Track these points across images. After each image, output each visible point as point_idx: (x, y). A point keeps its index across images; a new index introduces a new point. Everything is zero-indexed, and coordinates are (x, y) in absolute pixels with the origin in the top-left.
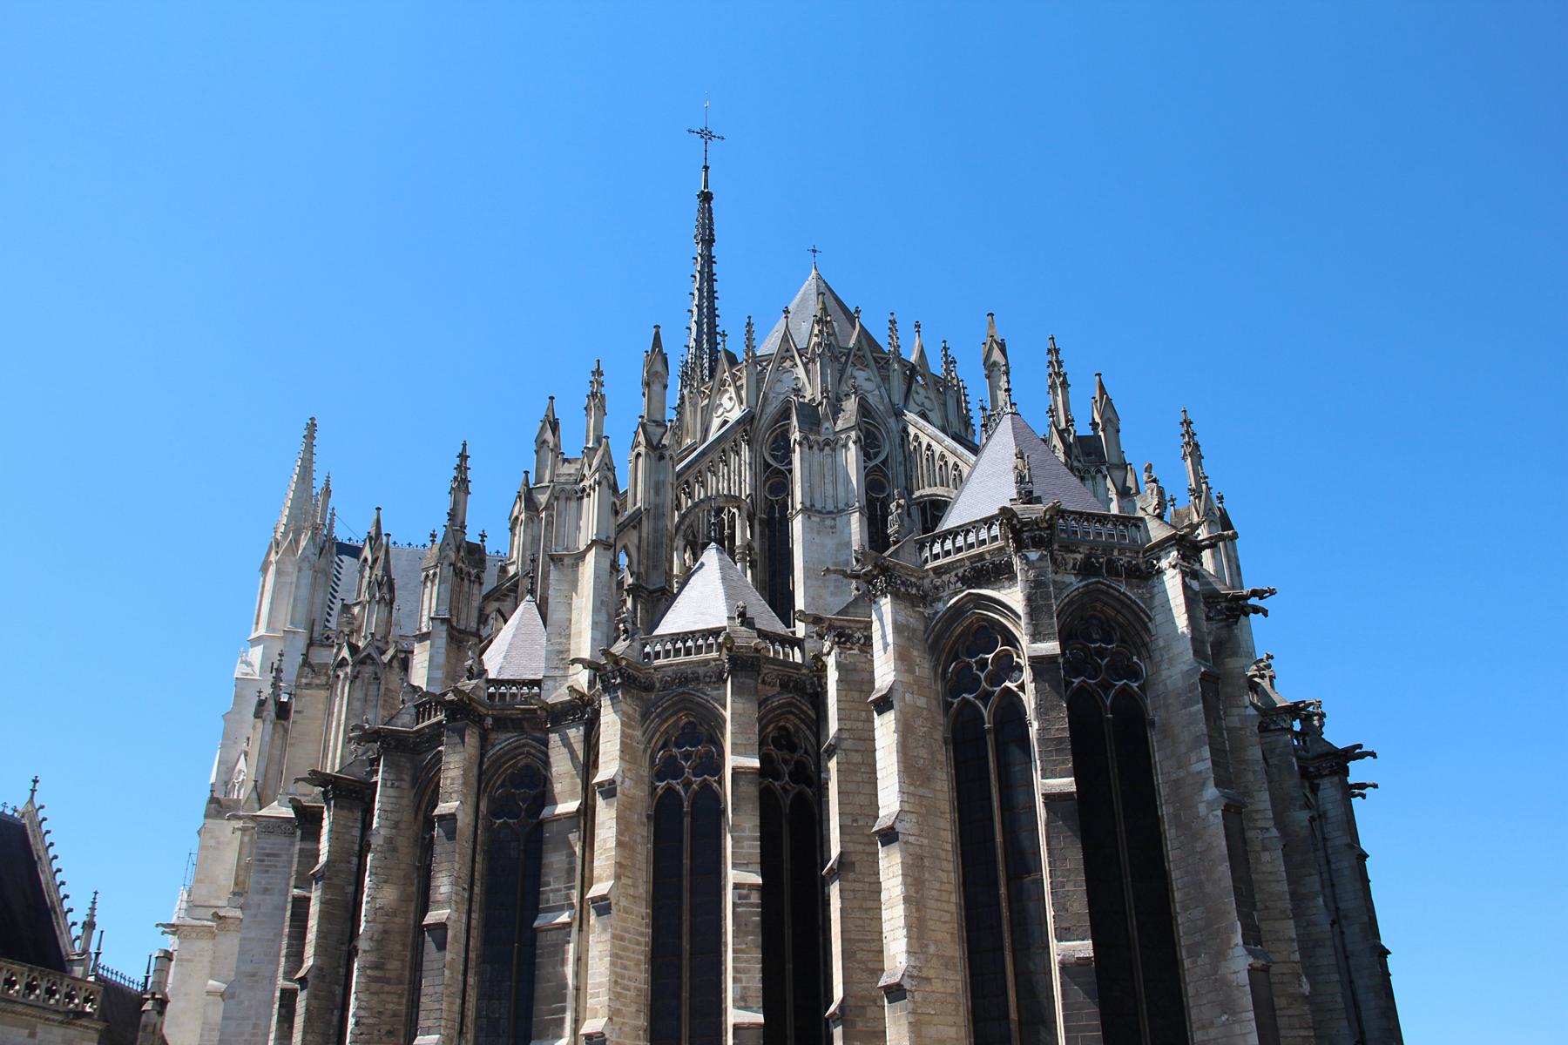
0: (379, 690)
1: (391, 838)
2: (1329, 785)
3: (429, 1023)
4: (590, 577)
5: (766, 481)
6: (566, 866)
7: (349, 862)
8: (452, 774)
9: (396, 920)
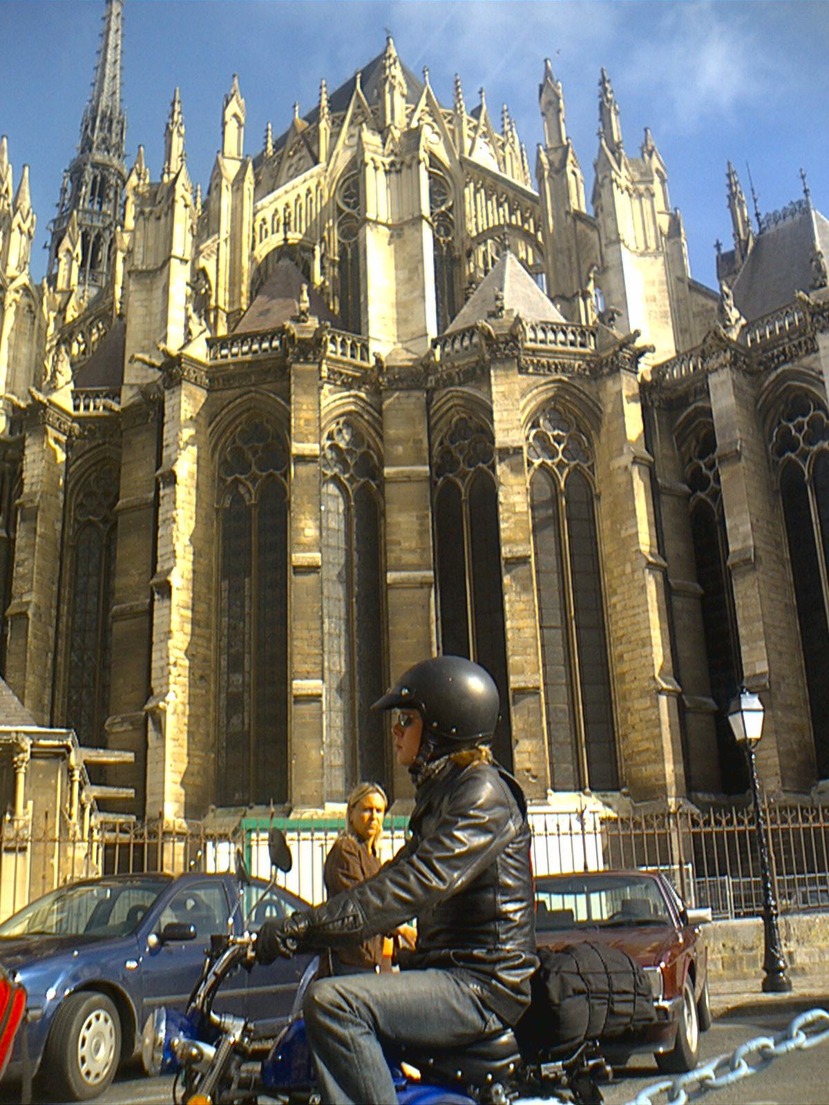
0: (33, 323)
3: (307, 667)
6: (416, 527)
7: (57, 497)
8: (304, 415)
9: (202, 560)
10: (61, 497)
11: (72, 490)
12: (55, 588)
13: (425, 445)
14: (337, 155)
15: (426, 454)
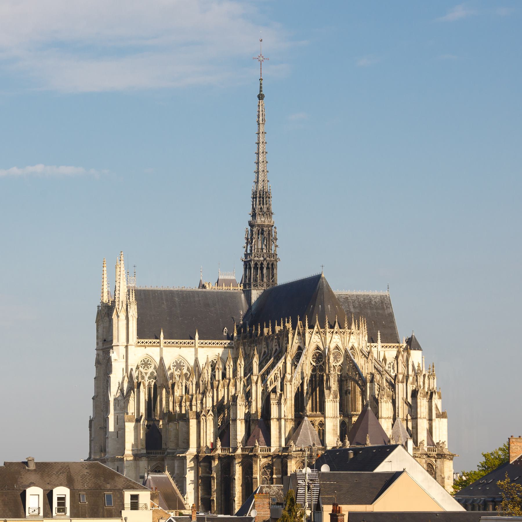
1: (239, 477)
2: (439, 461)
4: (272, 409)
5: (310, 369)
10: (220, 472)
11: (223, 470)
12: (220, 492)
13: (281, 471)
14: (294, 346)
15: (281, 473)
